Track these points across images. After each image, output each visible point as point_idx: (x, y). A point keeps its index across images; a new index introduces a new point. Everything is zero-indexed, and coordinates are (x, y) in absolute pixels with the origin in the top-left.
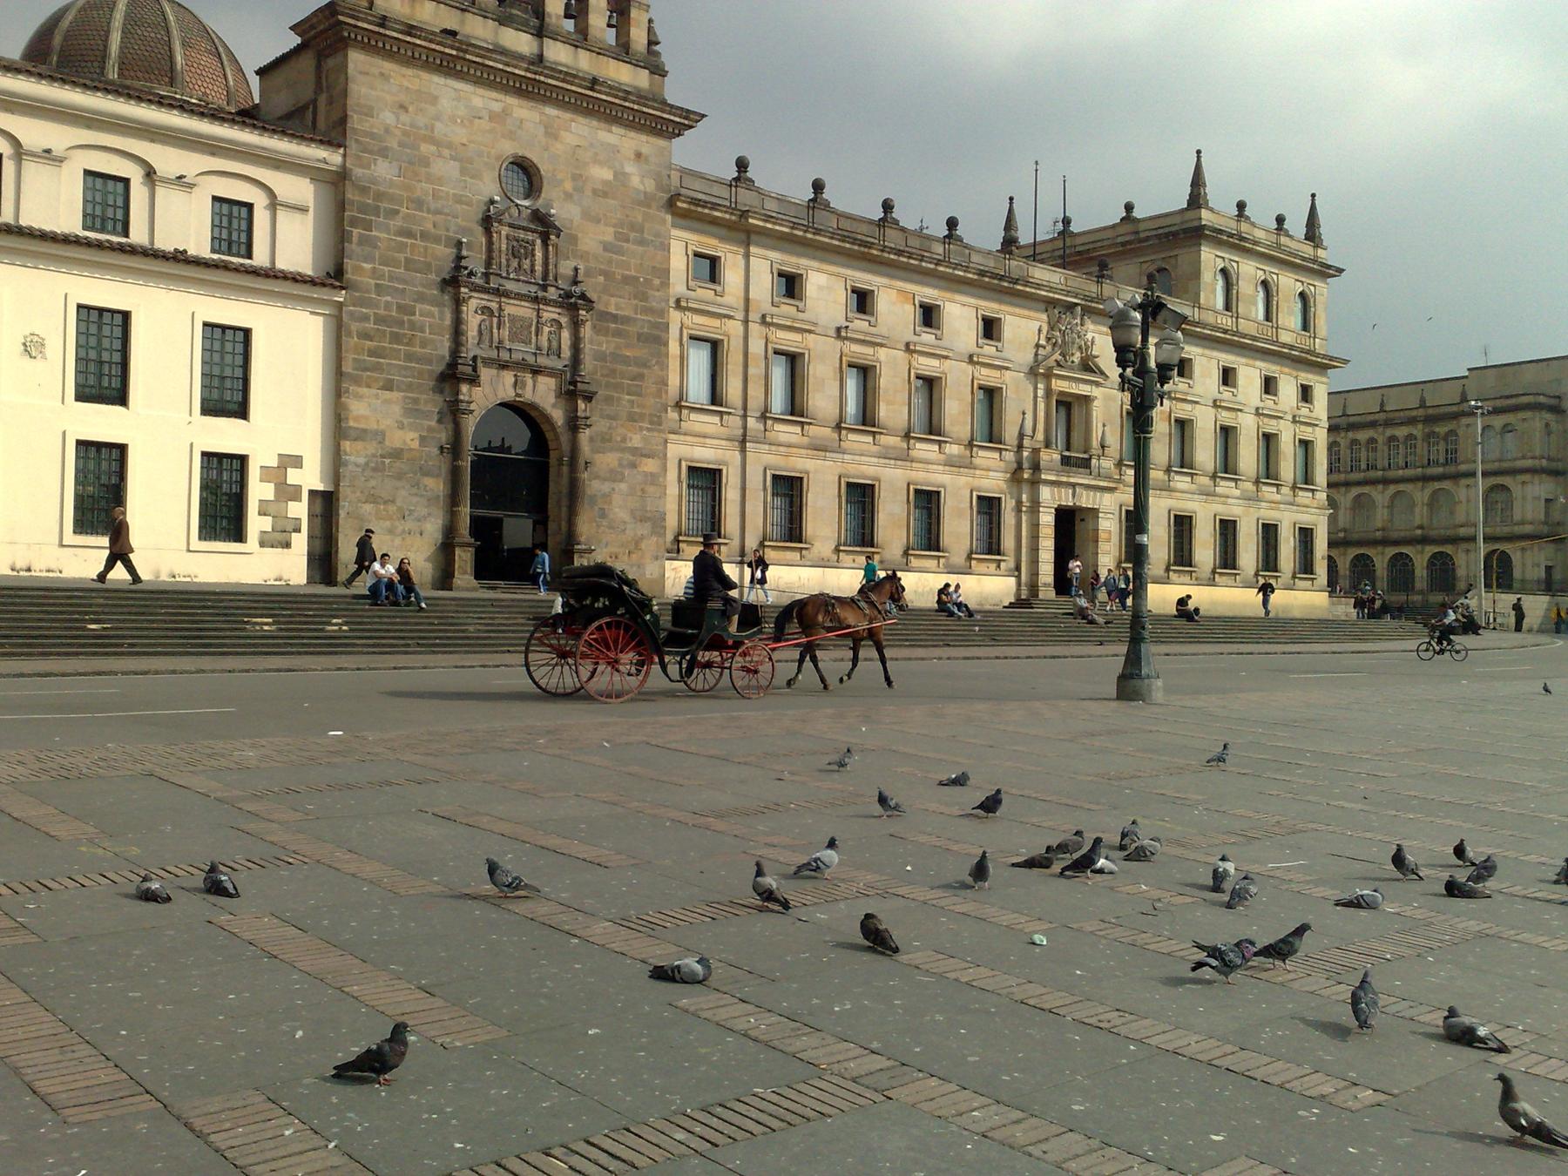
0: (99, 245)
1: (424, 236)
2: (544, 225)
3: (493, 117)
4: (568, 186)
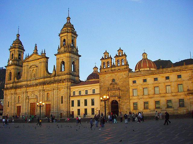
0: (86, 95)
1: (105, 88)
2: (116, 84)
3: (111, 76)
4: (118, 79)
